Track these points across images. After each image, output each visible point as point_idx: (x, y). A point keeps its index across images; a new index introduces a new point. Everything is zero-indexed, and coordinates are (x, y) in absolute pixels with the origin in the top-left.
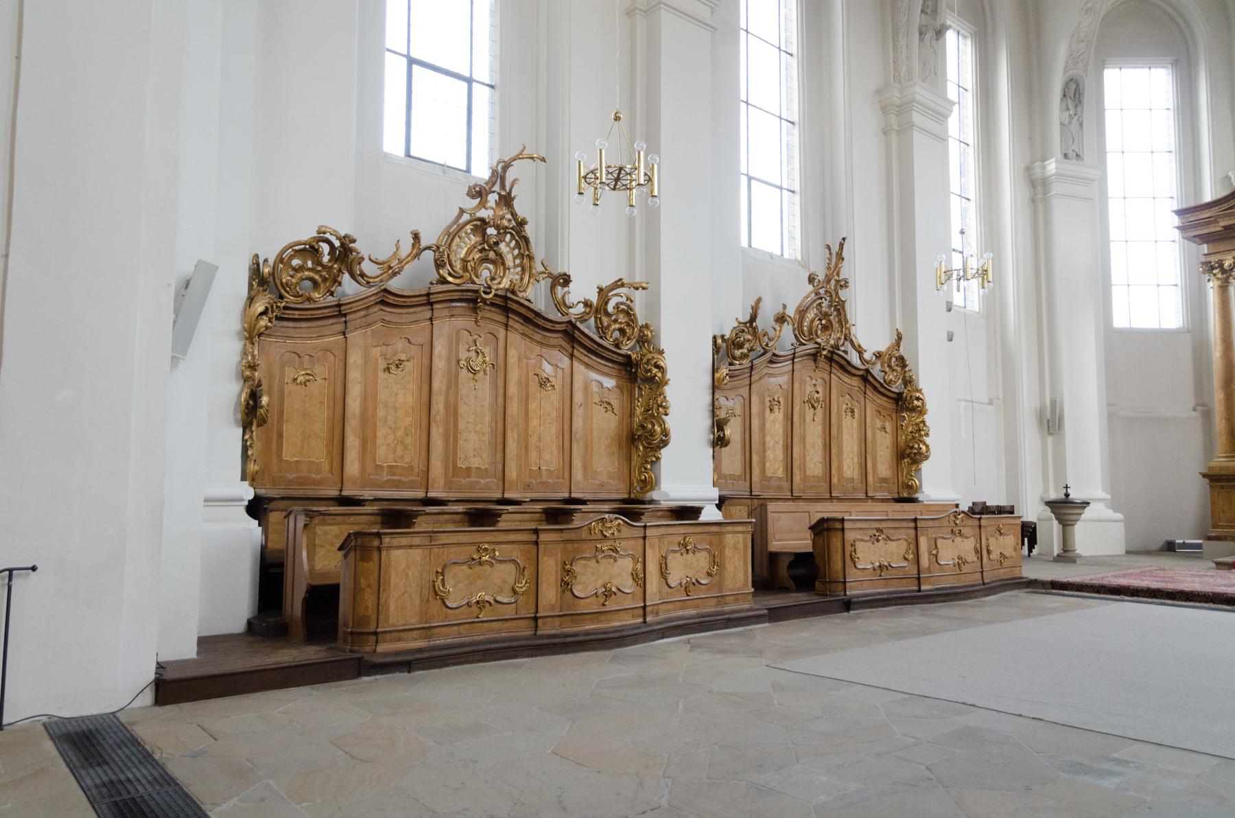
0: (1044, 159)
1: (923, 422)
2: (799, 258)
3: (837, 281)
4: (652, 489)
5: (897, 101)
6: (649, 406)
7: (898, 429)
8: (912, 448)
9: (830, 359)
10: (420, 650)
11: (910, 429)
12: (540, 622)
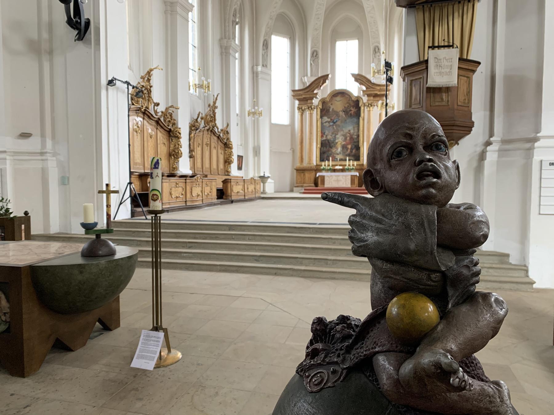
0: (257, 66)
1: (232, 152)
2: (198, 95)
3: (215, 106)
4: (177, 170)
5: (225, 45)
6: (175, 145)
7: (225, 153)
8: (229, 160)
9: (211, 131)
10: (169, 208)
11: (228, 154)
12: (187, 202)
